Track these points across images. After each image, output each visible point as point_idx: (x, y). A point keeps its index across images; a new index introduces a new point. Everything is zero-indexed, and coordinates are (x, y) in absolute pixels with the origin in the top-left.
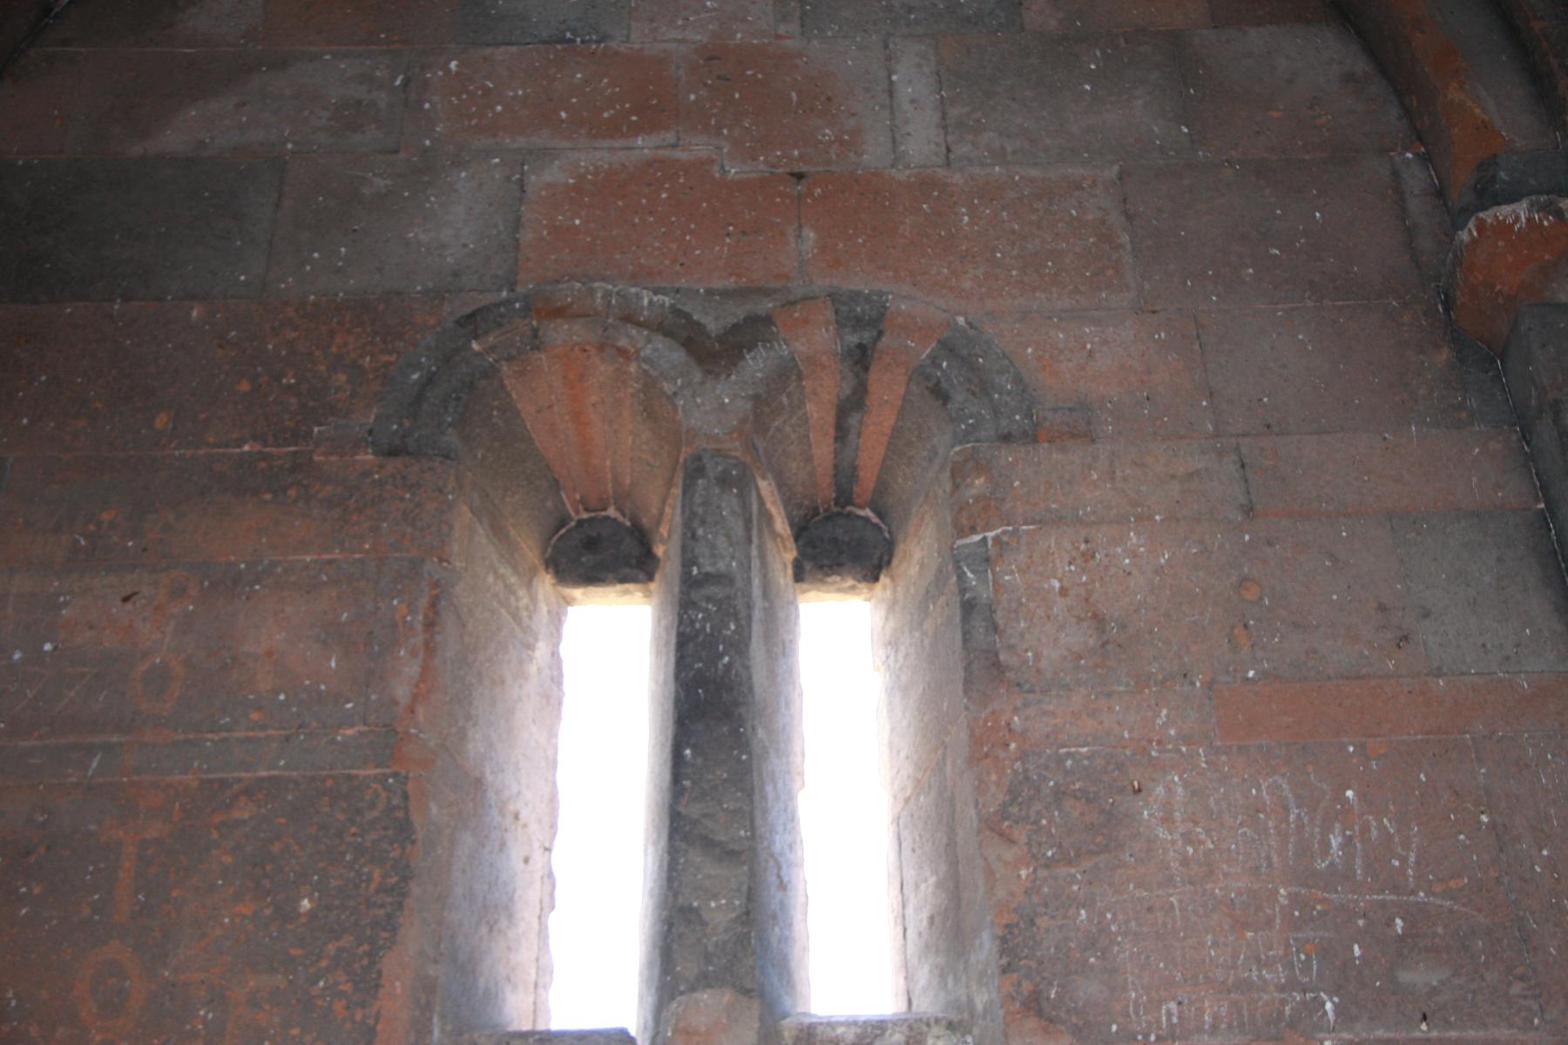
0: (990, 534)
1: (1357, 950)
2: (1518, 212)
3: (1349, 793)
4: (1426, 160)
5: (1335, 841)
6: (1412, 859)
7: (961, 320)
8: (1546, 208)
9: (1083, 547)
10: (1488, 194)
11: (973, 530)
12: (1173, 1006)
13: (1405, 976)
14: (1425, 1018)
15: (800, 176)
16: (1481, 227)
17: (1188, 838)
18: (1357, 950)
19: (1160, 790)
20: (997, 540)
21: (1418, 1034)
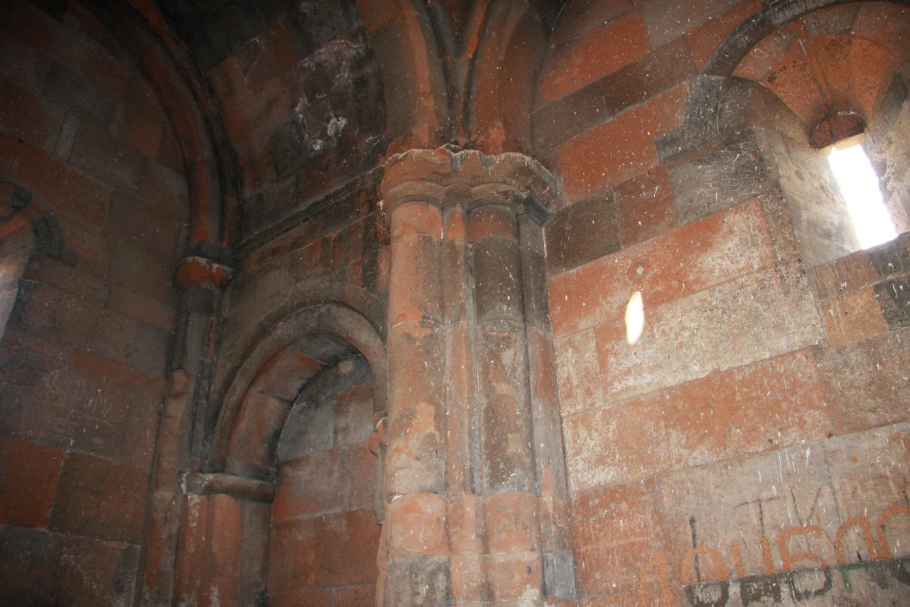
0: (34, 282)
1: (84, 430)
2: (203, 261)
3: (99, 390)
4: (189, 228)
5: (91, 401)
6: (107, 411)
7: (52, 213)
8: (210, 264)
9: (59, 297)
10: (198, 252)
11: (29, 278)
12: (32, 432)
13: (93, 440)
14: (93, 451)
15: (21, 141)
16: (194, 259)
17: (54, 389)
18: (84, 430)
19: (52, 373)
20: (35, 285)
21: (90, 454)
